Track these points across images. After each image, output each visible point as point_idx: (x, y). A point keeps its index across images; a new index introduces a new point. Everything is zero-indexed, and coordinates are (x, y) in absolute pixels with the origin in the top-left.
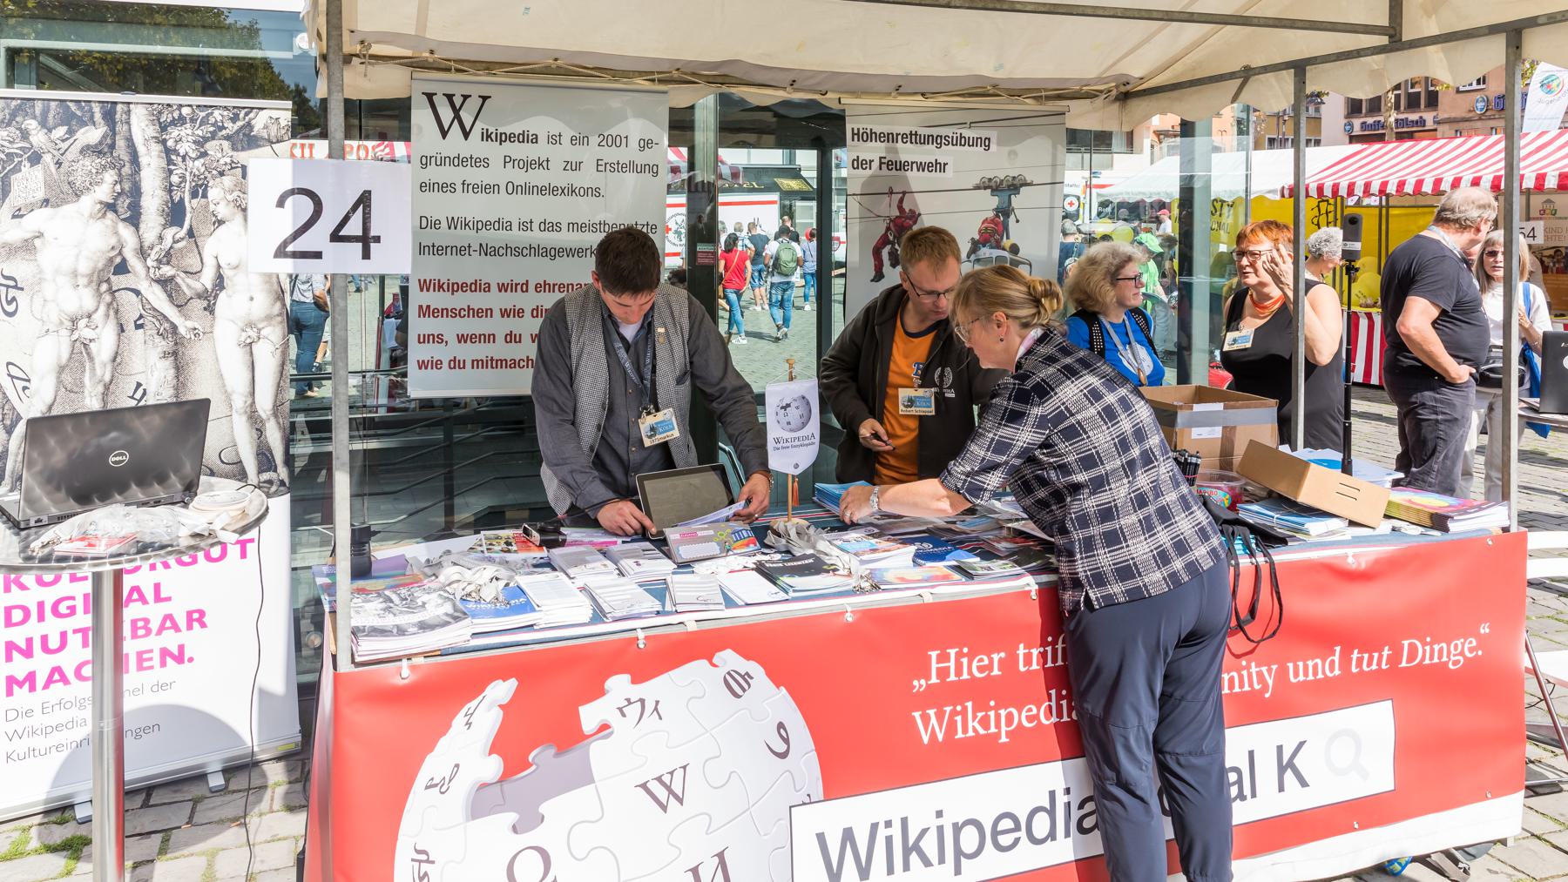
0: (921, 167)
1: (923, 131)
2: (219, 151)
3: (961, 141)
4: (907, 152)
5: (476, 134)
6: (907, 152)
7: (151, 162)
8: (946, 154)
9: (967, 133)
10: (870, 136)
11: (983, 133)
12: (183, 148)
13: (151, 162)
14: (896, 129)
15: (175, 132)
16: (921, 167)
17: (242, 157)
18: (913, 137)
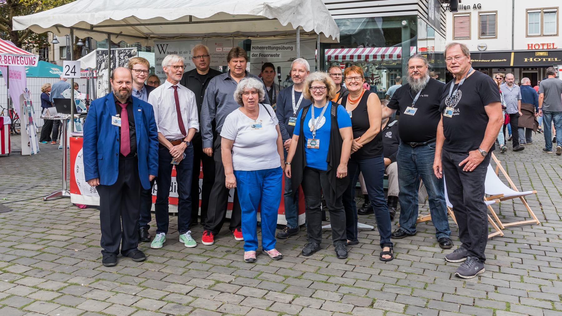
0: (272, 56)
1: (272, 46)
2: (127, 58)
3: (284, 48)
4: (267, 52)
5: (166, 53)
6: (267, 52)
7: (117, 60)
8: (280, 52)
9: (285, 46)
10: (258, 48)
11: (290, 46)
12: (122, 58)
13: (117, 60)
14: (264, 46)
15: (121, 55)
16: (272, 56)
17: (130, 59)
18: (269, 48)
